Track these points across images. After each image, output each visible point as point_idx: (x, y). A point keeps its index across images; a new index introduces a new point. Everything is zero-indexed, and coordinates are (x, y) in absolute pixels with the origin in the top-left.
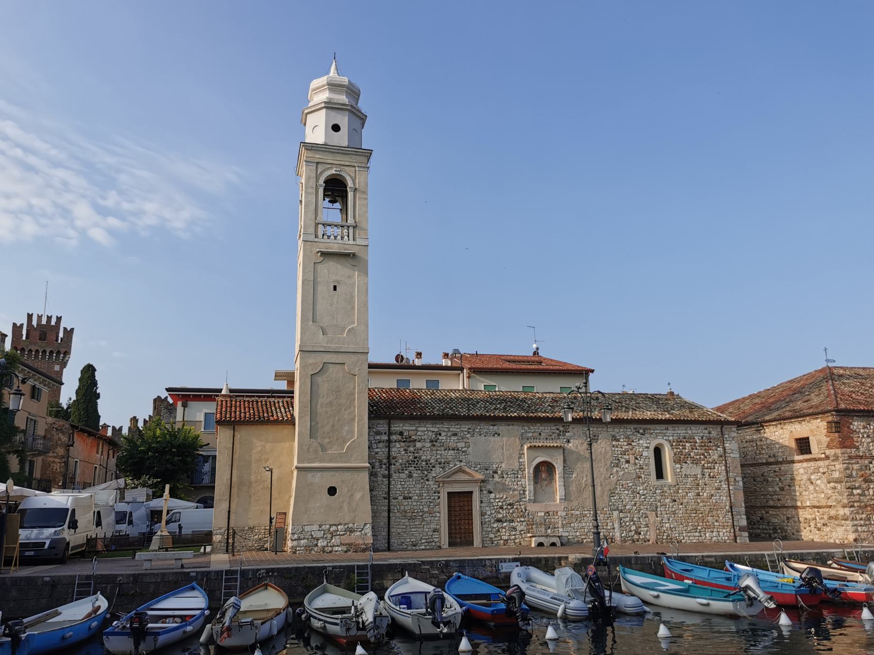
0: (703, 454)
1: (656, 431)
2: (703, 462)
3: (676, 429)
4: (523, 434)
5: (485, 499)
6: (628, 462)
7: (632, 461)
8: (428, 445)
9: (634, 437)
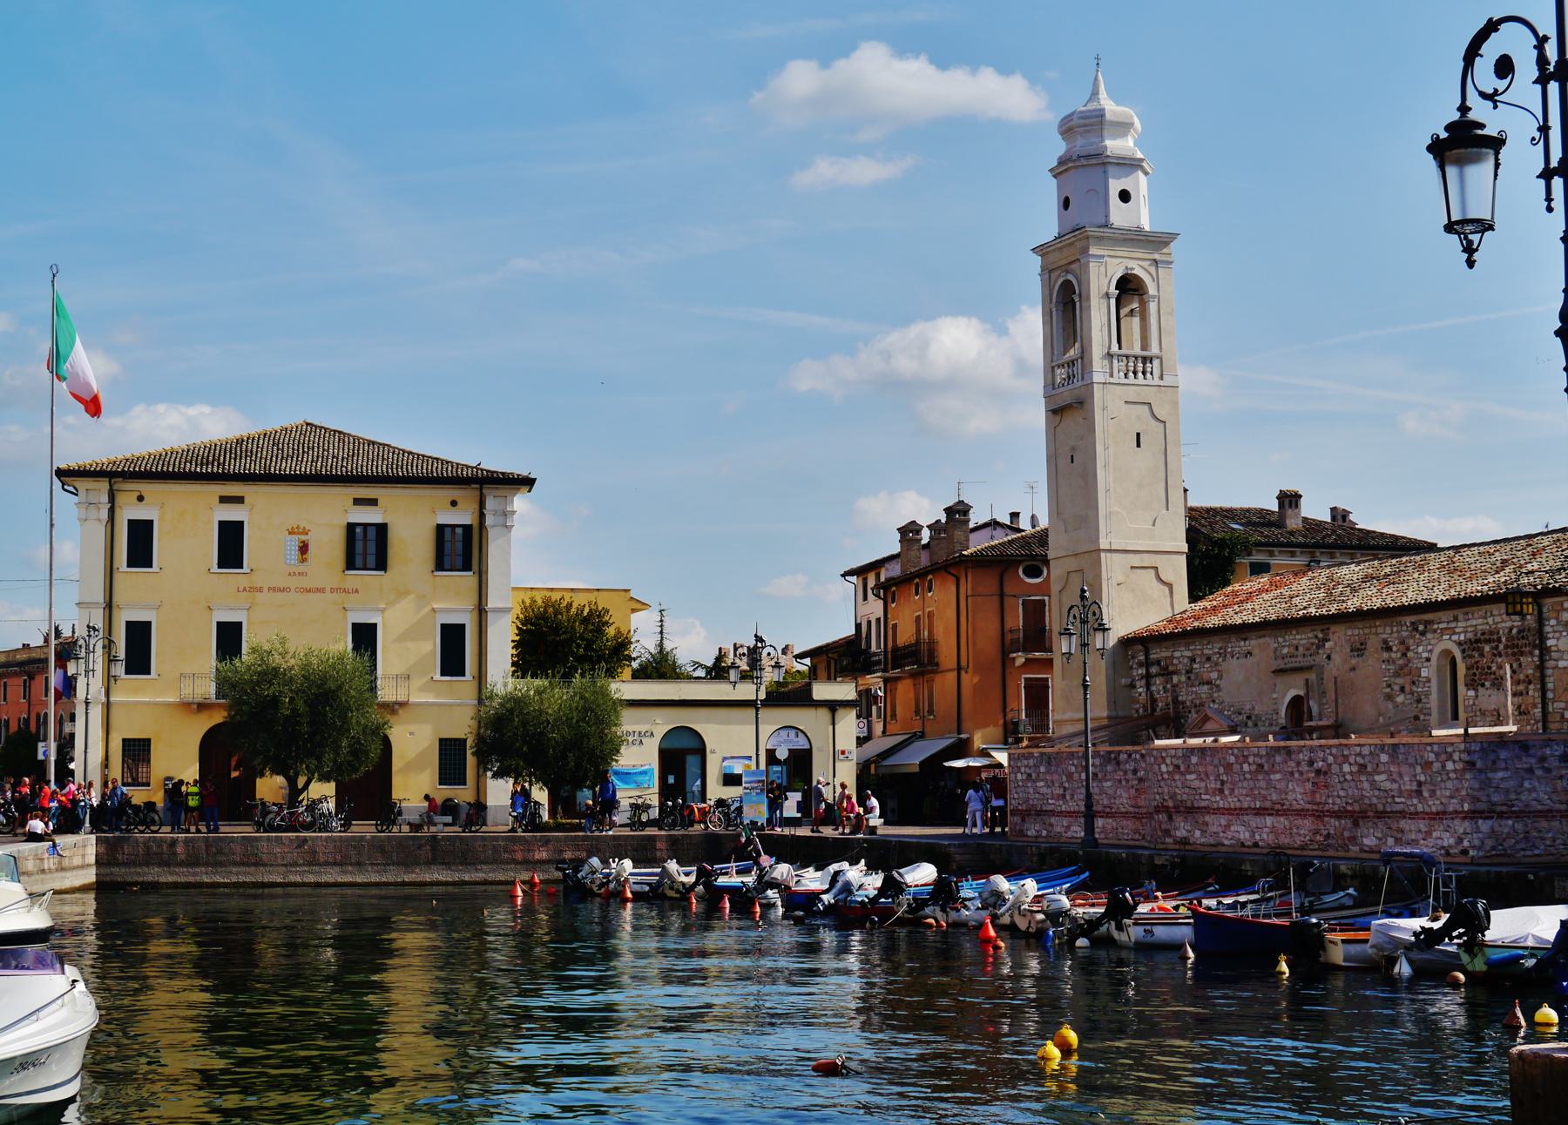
1: (1442, 626)
3: (1470, 616)
4: (1276, 649)
6: (1402, 689)
7: (1407, 689)
8: (1183, 679)
9: (1411, 641)
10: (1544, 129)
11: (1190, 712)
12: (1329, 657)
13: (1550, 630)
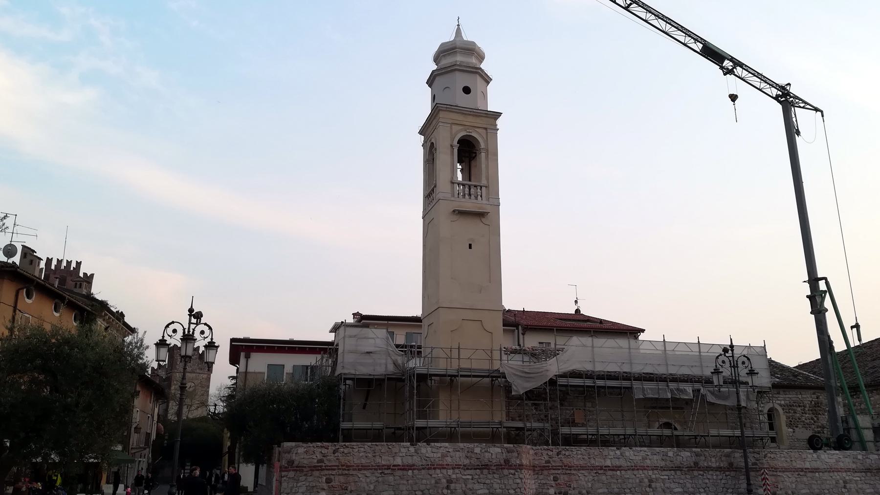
0: (812, 419)
2: (813, 426)
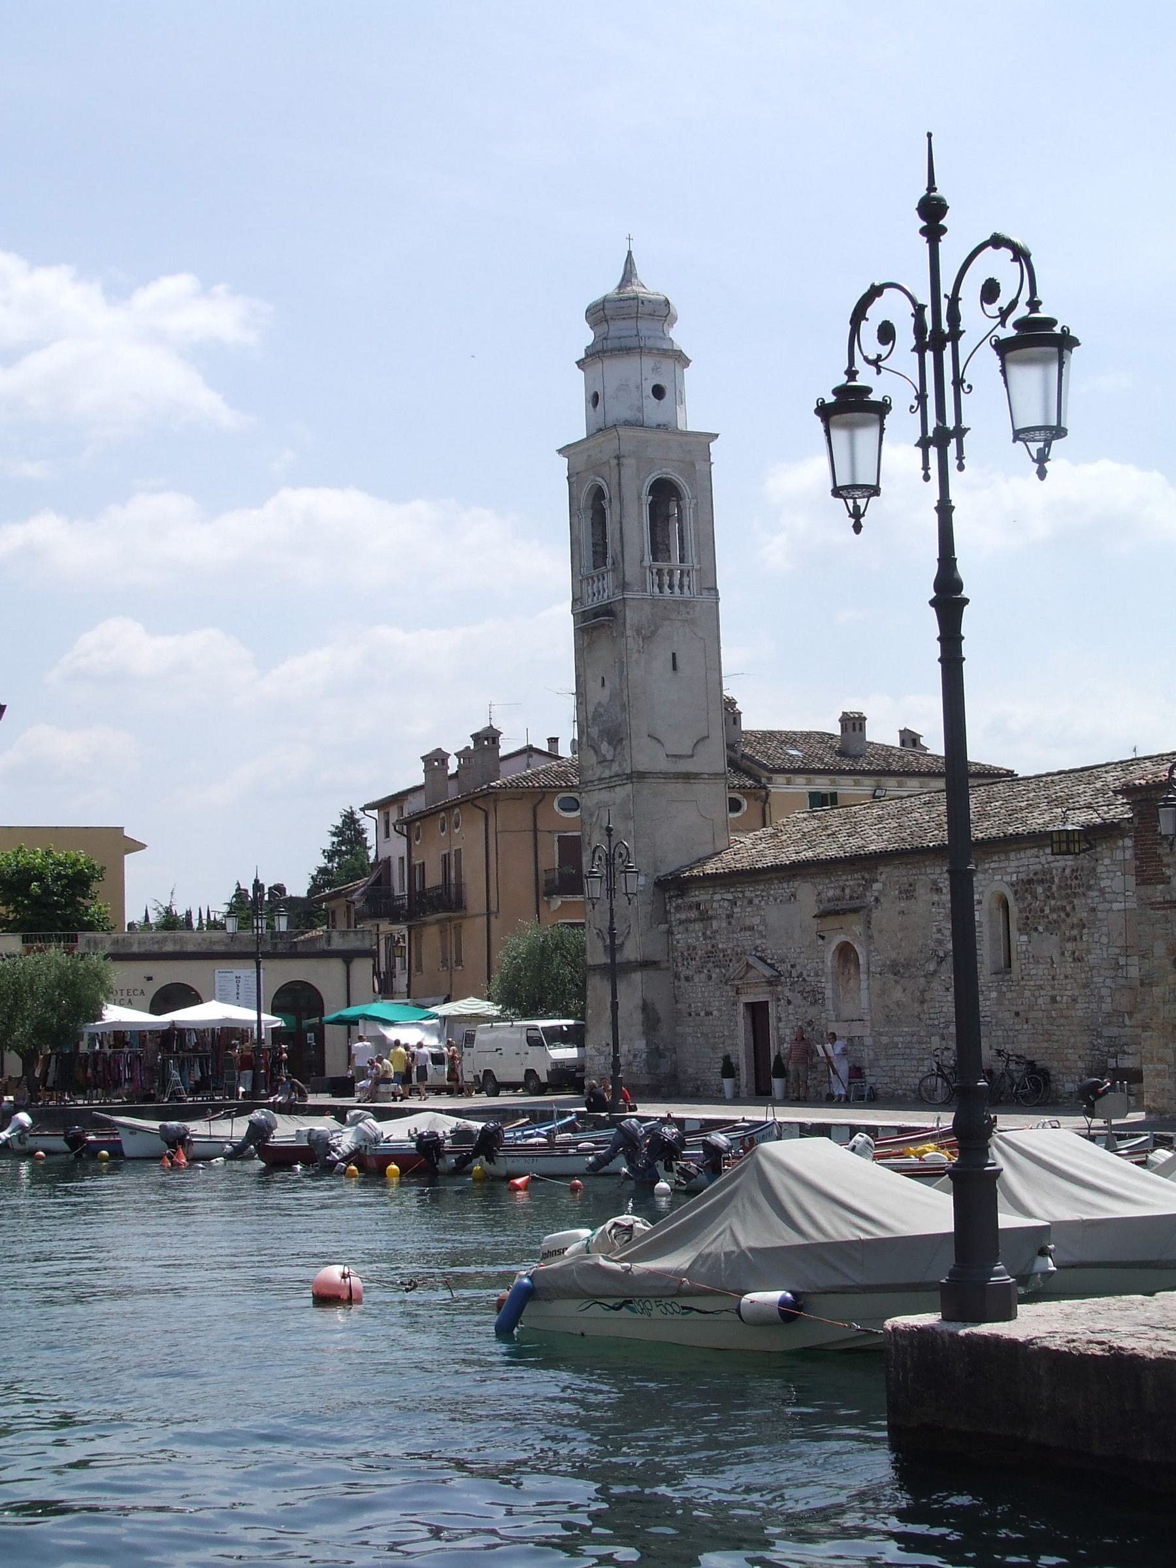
0: (1063, 908)
5: (783, 1015)
8: (724, 925)
10: (921, 398)
11: (731, 960)
12: (877, 900)
13: (1104, 869)
